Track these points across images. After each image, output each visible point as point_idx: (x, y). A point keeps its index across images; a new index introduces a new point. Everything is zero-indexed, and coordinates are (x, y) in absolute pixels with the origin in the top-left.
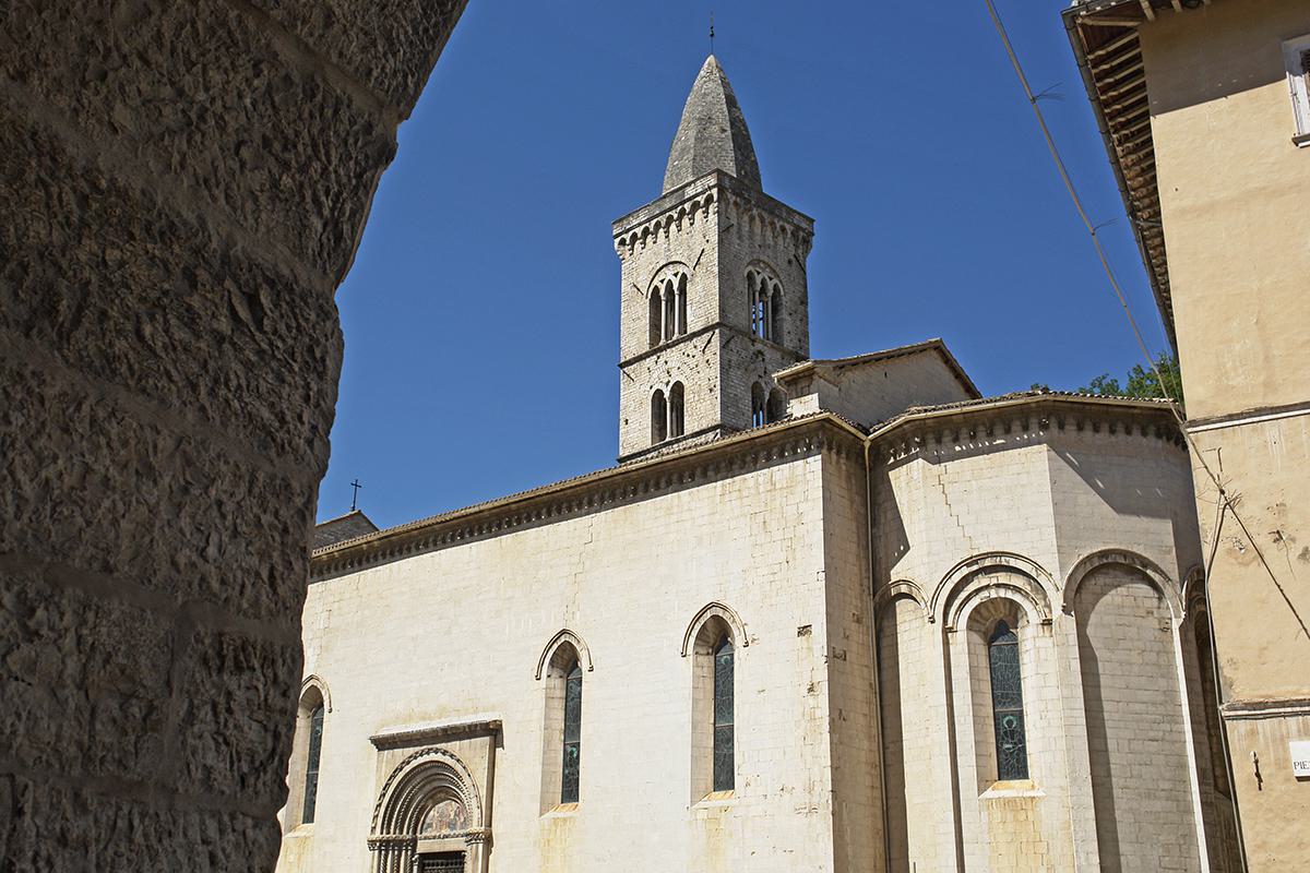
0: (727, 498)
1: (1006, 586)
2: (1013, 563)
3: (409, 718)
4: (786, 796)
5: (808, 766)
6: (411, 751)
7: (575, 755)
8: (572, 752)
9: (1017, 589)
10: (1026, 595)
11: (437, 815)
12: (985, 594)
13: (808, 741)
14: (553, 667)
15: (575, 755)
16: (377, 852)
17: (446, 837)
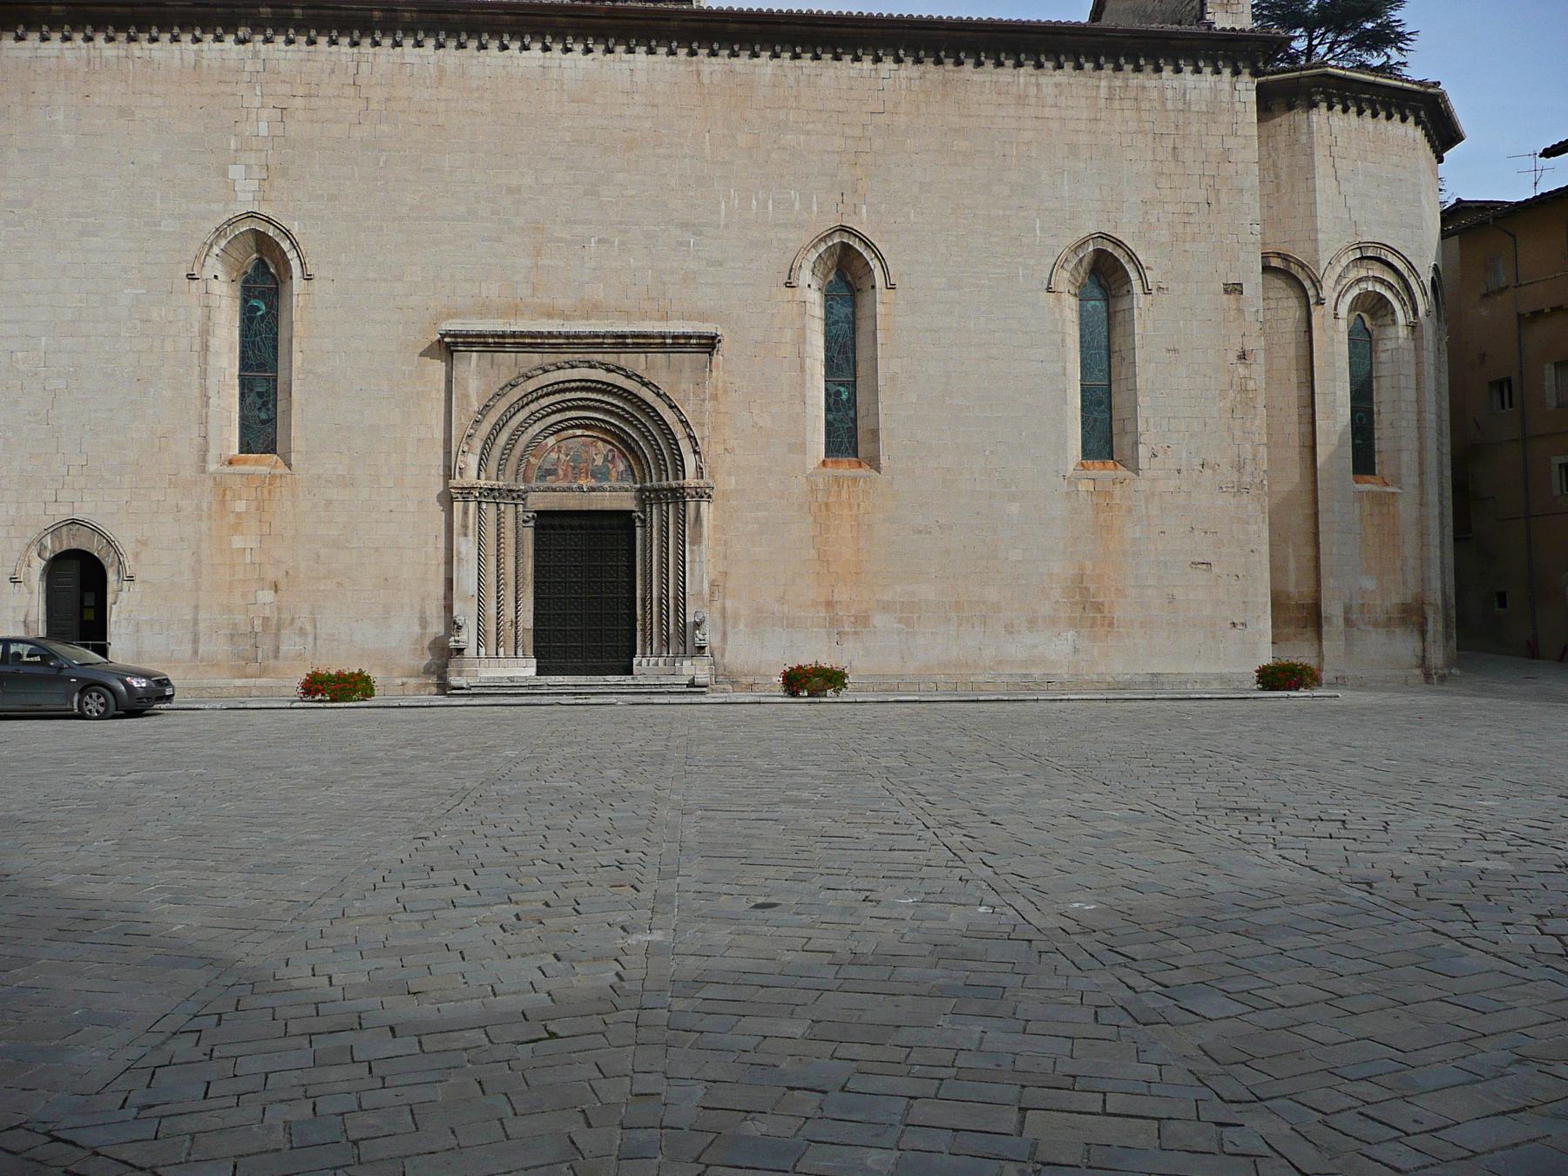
0: (1116, 104)
1: (1382, 281)
2: (1391, 259)
3: (515, 311)
4: (1208, 472)
5: (1237, 442)
6: (537, 359)
7: (844, 397)
8: (838, 393)
9: (1390, 287)
10: (1397, 294)
11: (562, 457)
12: (1363, 285)
13: (1238, 414)
14: (813, 274)
15: (844, 397)
16: (472, 506)
17: (593, 489)
